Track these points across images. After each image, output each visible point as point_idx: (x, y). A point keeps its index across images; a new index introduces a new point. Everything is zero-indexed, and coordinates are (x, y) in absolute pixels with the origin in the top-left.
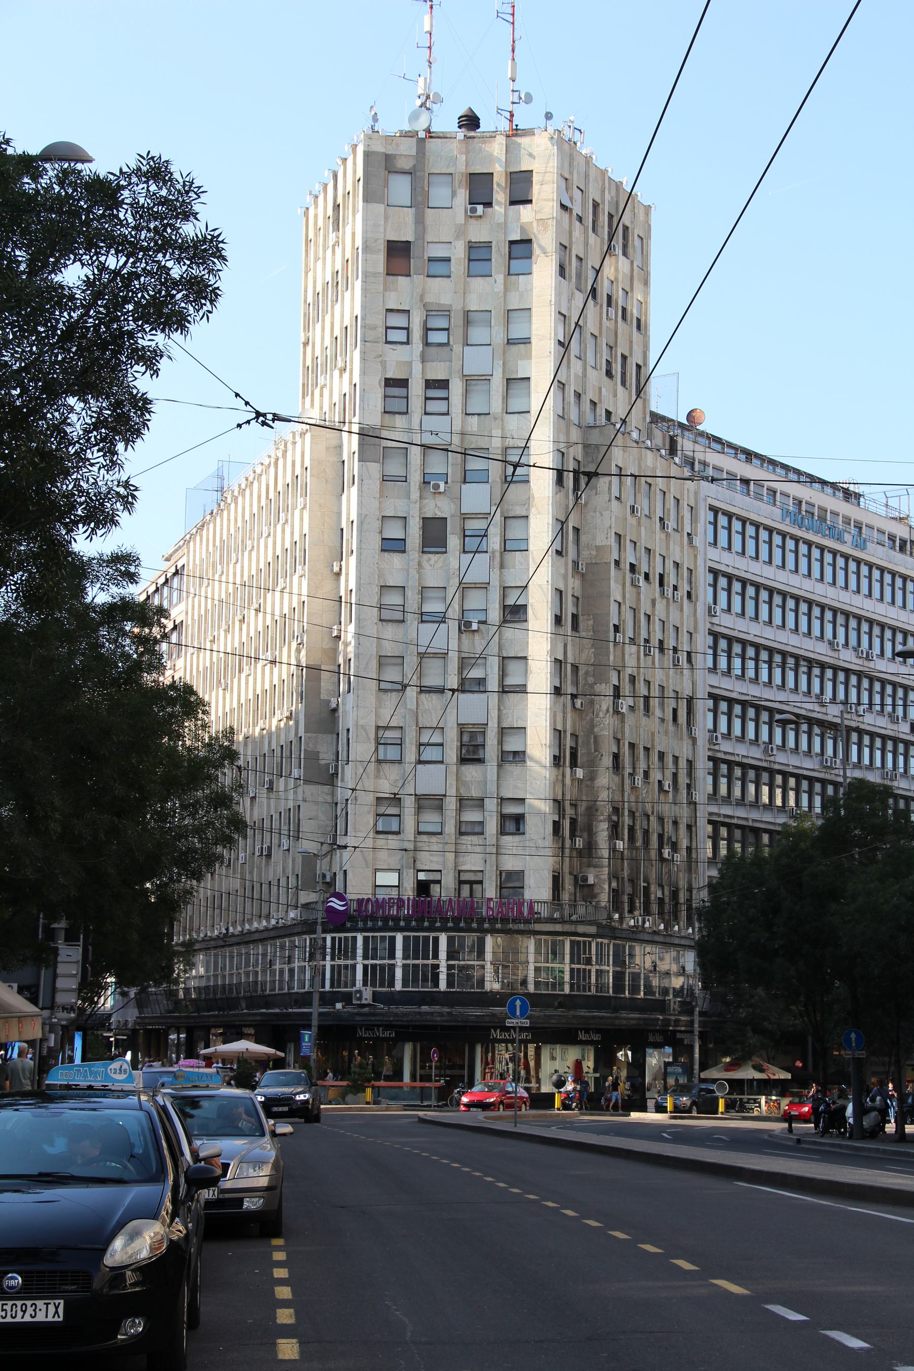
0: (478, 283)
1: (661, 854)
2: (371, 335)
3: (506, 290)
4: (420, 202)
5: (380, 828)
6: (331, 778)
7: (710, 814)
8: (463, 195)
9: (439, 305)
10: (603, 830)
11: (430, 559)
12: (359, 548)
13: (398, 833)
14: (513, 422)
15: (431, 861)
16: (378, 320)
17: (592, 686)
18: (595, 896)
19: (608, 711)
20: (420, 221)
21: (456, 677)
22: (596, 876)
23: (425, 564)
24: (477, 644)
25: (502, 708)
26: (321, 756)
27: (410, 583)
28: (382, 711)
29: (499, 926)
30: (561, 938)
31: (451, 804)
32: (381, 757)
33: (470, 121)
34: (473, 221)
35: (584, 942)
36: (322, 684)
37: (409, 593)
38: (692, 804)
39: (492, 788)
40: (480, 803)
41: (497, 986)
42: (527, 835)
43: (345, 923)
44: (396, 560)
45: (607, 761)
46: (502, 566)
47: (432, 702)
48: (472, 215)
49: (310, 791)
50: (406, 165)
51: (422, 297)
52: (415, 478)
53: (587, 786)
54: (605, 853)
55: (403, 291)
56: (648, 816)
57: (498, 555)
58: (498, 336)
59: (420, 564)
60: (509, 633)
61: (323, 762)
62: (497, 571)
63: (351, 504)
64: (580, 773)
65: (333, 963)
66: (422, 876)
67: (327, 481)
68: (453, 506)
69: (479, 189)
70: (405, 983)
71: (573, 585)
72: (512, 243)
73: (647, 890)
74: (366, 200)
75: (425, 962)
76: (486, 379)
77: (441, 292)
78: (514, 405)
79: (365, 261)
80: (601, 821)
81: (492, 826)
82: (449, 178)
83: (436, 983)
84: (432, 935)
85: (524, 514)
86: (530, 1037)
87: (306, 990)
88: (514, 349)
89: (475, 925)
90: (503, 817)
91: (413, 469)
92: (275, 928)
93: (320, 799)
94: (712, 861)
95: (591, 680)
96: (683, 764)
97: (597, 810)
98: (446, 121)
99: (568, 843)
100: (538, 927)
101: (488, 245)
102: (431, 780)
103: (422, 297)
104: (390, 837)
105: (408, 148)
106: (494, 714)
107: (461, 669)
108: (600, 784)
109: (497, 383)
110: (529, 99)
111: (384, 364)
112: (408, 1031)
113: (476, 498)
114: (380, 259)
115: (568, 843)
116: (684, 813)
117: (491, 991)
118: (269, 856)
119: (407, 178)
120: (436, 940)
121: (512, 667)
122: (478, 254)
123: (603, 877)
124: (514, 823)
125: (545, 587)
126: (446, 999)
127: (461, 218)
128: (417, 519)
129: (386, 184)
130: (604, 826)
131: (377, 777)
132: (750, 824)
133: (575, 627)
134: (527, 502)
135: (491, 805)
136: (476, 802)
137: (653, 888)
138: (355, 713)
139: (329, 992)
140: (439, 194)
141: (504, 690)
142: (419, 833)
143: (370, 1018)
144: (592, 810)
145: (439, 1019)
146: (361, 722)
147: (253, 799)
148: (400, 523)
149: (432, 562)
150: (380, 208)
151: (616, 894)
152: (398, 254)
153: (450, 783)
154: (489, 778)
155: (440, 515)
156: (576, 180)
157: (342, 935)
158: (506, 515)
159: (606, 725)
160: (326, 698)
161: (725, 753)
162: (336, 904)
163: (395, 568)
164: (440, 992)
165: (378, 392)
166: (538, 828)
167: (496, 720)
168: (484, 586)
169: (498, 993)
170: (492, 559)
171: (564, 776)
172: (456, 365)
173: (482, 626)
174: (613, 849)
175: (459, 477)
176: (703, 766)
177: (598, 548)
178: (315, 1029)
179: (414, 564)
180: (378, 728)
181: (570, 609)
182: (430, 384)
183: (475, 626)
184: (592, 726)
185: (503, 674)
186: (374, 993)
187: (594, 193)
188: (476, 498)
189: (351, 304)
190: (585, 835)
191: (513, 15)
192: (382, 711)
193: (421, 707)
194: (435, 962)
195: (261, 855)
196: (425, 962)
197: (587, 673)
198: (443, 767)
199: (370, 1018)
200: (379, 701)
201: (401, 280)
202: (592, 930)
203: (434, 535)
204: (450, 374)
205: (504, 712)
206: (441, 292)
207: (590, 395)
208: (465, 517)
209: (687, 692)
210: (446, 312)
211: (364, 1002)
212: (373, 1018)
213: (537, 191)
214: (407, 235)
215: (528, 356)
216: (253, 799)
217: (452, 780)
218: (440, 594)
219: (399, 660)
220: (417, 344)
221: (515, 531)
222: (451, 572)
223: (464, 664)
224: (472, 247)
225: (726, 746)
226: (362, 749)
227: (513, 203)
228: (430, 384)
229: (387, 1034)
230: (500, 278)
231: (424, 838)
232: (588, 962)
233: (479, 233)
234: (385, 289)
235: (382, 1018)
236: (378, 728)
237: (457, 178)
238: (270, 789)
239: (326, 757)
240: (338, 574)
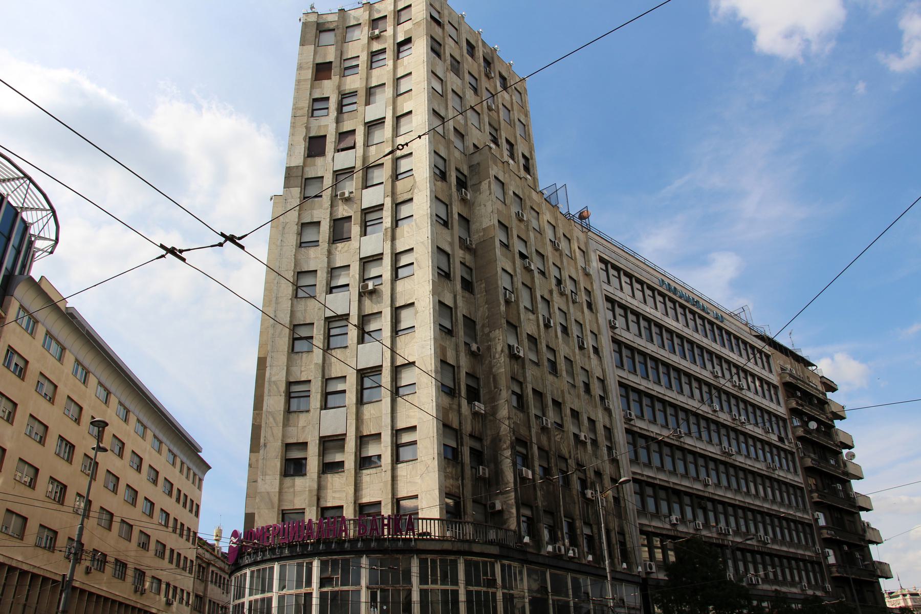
1: (584, 495)
2: (299, 113)
7: (634, 473)
15: (334, 498)
17: (488, 335)
18: (505, 522)
19: (502, 351)
30: (453, 557)
35: (485, 563)
38: (615, 461)
54: (509, 476)
56: (566, 460)
57: (389, 230)
64: (480, 407)
73: (571, 526)
85: (409, 197)
95: (487, 330)
96: (601, 431)
97: (500, 440)
99: (468, 472)
102: (336, 421)
106: (388, 354)
114: (309, 74)
115: (468, 472)
116: (608, 469)
121: (404, 314)
123: (510, 502)
125: (426, 243)
130: (508, 453)
132: (671, 486)
137: (578, 523)
146: (273, 379)
149: (339, 249)
161: (641, 428)
167: (389, 360)
170: (385, 234)
171: (459, 406)
174: (521, 480)
176: (620, 437)
177: (484, 230)
190: (492, 466)
197: (483, 326)
202: (494, 550)
221: (405, 211)
225: (640, 424)
232: (492, 583)
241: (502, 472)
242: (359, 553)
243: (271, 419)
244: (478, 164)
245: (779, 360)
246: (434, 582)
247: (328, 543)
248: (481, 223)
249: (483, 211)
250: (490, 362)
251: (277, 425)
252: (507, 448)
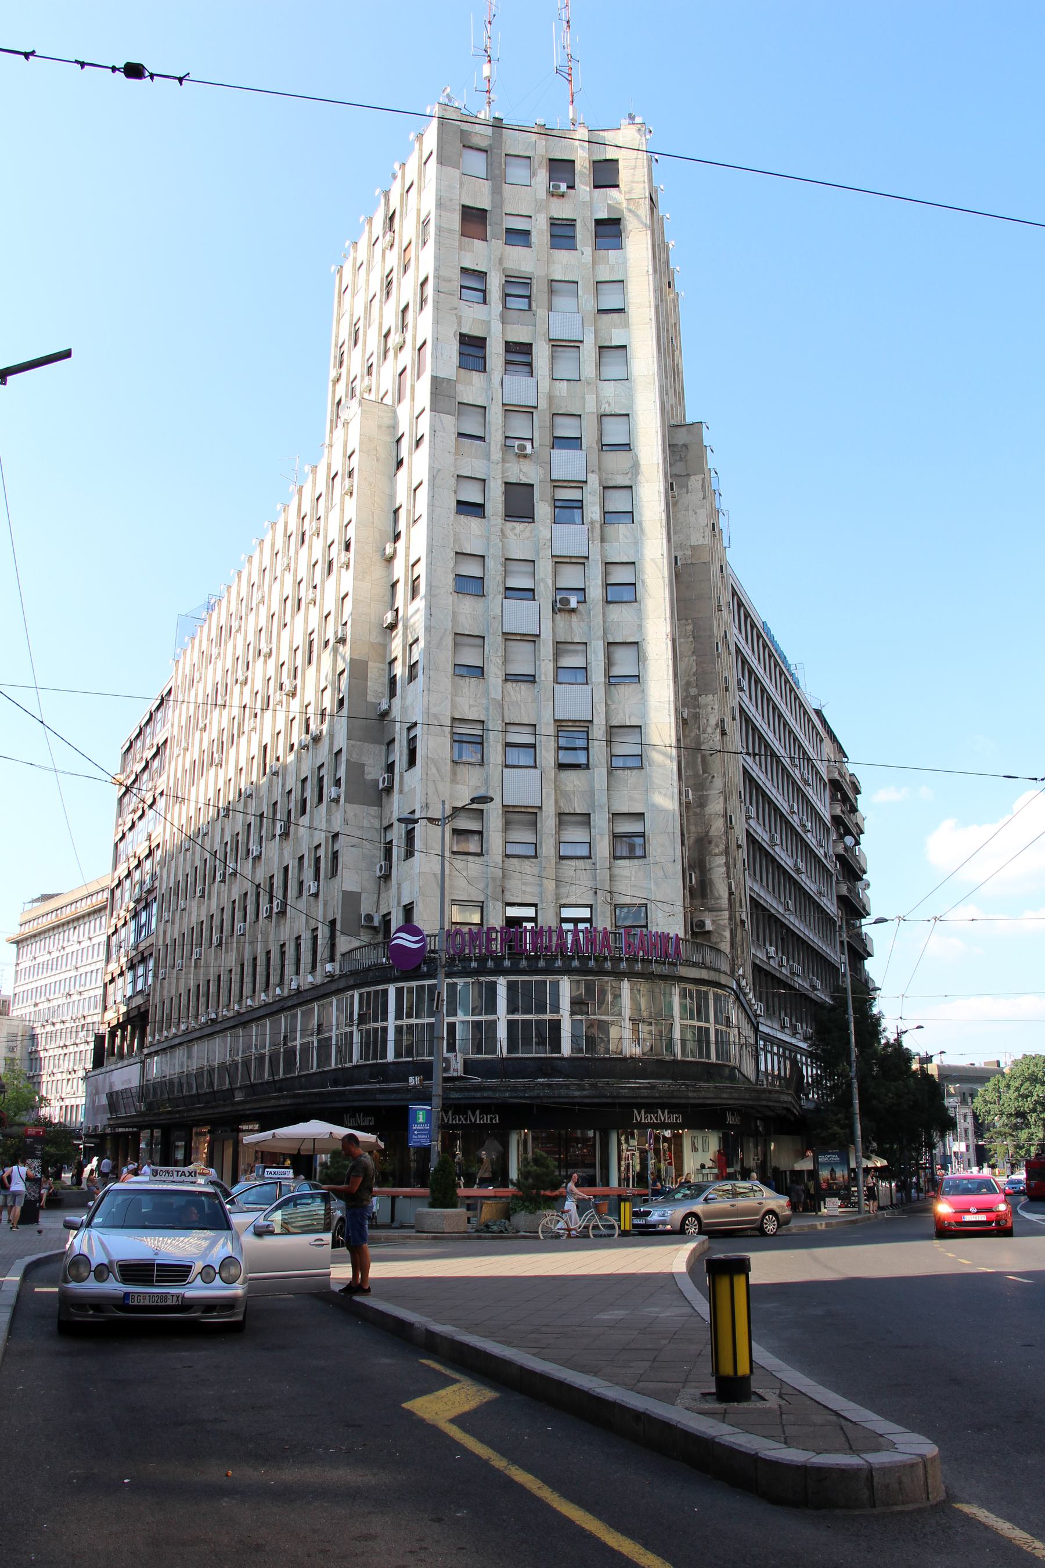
0: (563, 256)
3: (594, 263)
4: (496, 177)
5: (455, 849)
8: (543, 175)
9: (519, 271)
10: (719, 866)
11: (514, 529)
12: (431, 506)
13: (481, 854)
14: (608, 390)
15: (524, 892)
17: (695, 698)
20: (497, 192)
21: (551, 664)
22: (713, 922)
23: (508, 532)
24: (575, 629)
25: (609, 703)
26: (367, 769)
27: (492, 551)
28: (458, 699)
29: (638, 967)
30: (704, 988)
31: (548, 821)
32: (456, 759)
34: (555, 200)
36: (369, 684)
37: (490, 563)
39: (601, 798)
40: (585, 819)
41: (636, 1051)
42: (651, 859)
43: (419, 966)
44: (474, 524)
46: (602, 540)
47: (519, 692)
48: (554, 194)
49: (353, 809)
50: (483, 143)
51: (501, 261)
52: (496, 438)
53: (696, 814)
55: (478, 254)
57: (598, 526)
58: (588, 303)
59: (502, 530)
60: (619, 614)
61: (369, 777)
62: (597, 543)
63: (419, 465)
65: (399, 1023)
66: (513, 912)
67: (378, 460)
68: (541, 471)
69: (561, 169)
70: (512, 1046)
72: (599, 222)
74: (440, 162)
75: (542, 1017)
76: (575, 345)
77: (522, 260)
78: (609, 372)
79: (439, 216)
80: (716, 855)
81: (603, 848)
82: (527, 161)
83: (556, 1046)
84: (549, 979)
85: (627, 483)
86: (680, 1121)
87: (354, 1063)
88: (606, 317)
89: (608, 965)
90: (616, 837)
91: (493, 429)
92: (299, 991)
93: (366, 824)
95: (693, 691)
97: (710, 842)
100: (684, 971)
101: (571, 224)
102: (522, 787)
103: (501, 261)
104: (470, 858)
106: (601, 708)
107: (557, 655)
108: (713, 811)
109: (589, 350)
111: (459, 319)
112: (514, 1115)
113: (567, 464)
114: (455, 220)
117: (631, 1058)
118: (282, 913)
119: (482, 156)
120: (556, 986)
121: (620, 654)
123: (721, 922)
124: (629, 845)
126: (576, 1067)
127: (542, 194)
128: (500, 482)
129: (460, 156)
130: (722, 860)
131: (454, 781)
134: (635, 468)
135: (600, 821)
136: (579, 818)
138: (426, 699)
139: (393, 1063)
140: (516, 173)
141: (611, 680)
142: (507, 856)
143: (473, 1094)
145: (577, 1093)
146: (433, 710)
147: (258, 858)
148: (478, 486)
149: (517, 531)
150: (456, 173)
152: (474, 220)
153: (548, 794)
154: (597, 786)
155: (524, 480)
157: (414, 984)
158: (605, 485)
160: (374, 700)
163: (473, 533)
164: (563, 1059)
165: (453, 347)
166: (666, 849)
167: (603, 716)
168: (581, 562)
169: (640, 1060)
172: (541, 328)
173: (581, 607)
175: (548, 441)
177: (693, 548)
178: (437, 1101)
179: (496, 531)
180: (454, 719)
182: (511, 347)
183: (573, 604)
185: (609, 663)
186: (466, 1062)
188: (567, 464)
191: (570, 75)
192: (458, 699)
193: (507, 699)
194: (555, 1017)
195: (269, 917)
196: (542, 1017)
198: (536, 773)
199: (473, 1094)
200: (453, 683)
201: (478, 243)
203: (519, 503)
204: (534, 338)
205: (613, 707)
206: (522, 260)
208: (557, 484)
210: (526, 282)
211: (452, 1074)
212: (478, 1095)
213: (624, 175)
214: (484, 203)
215: (626, 325)
216: (258, 858)
217: (549, 789)
218: (528, 567)
219: (479, 641)
222: (542, 542)
223: (560, 647)
224: (555, 223)
226: (434, 746)
227: (596, 187)
228: (511, 347)
229: (487, 1119)
230: (588, 250)
231: (515, 861)
233: (562, 210)
234: (461, 248)
235: (491, 1094)
236: (454, 719)
237: (536, 163)
238: (285, 835)
239: (375, 772)
240: (390, 560)
241: (711, 882)
242: (619, 975)
243: (434, 770)
244: (685, 446)
245: (828, 747)
246: (692, 1018)
247: (584, 960)
248: (688, 537)
249: (692, 519)
250: (698, 737)
251: (442, 779)
252: (721, 854)
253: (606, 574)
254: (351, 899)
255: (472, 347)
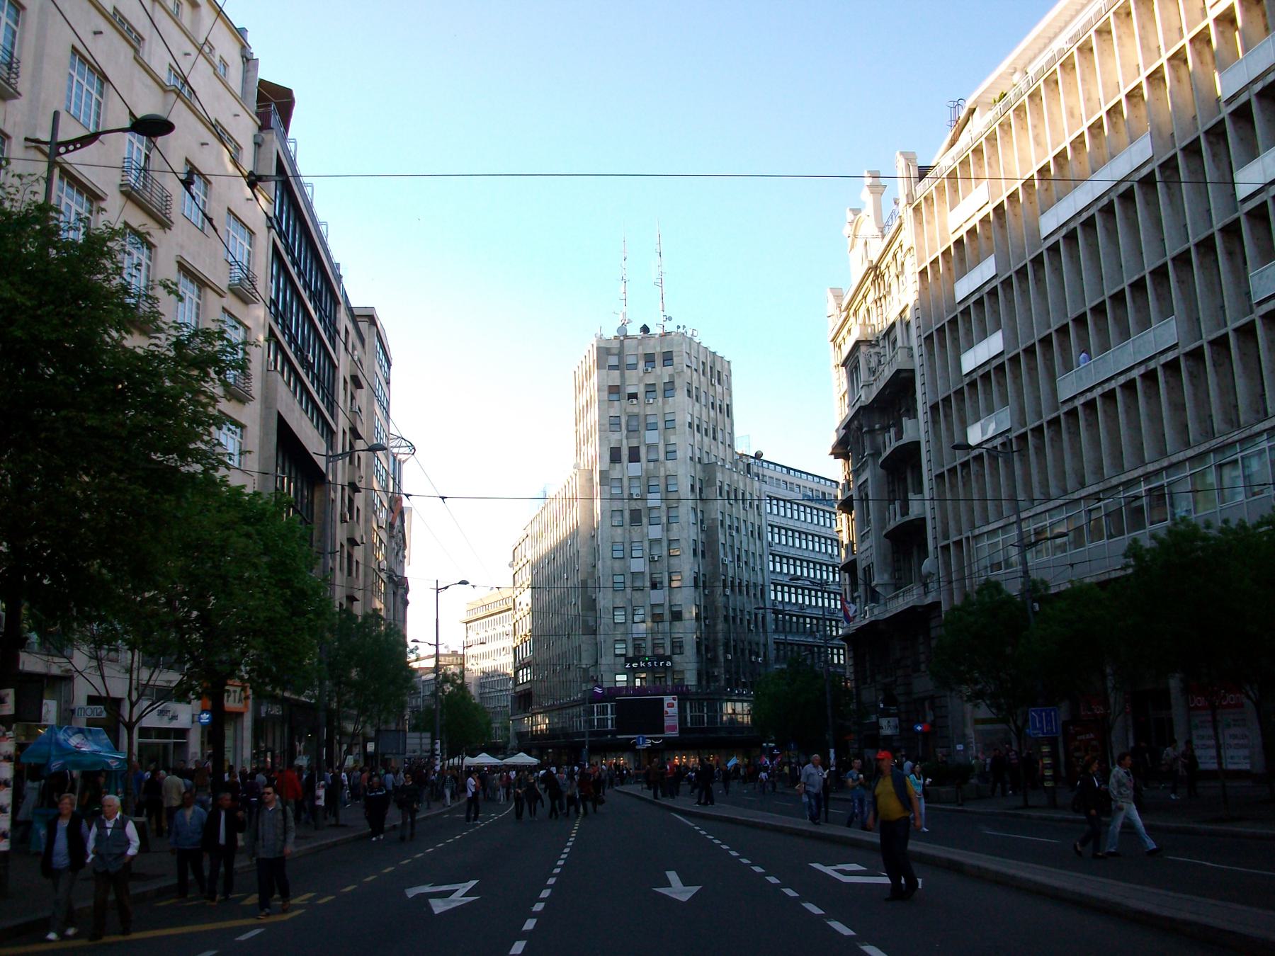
6: (594, 632)
16: (606, 422)
33: (645, 329)
45: (721, 619)
47: (638, 595)
48: (646, 372)
54: (722, 659)
71: (701, 537)
94: (777, 660)
98: (634, 330)
105: (616, 344)
110: (670, 319)
114: (605, 395)
122: (650, 389)
127: (641, 374)
133: (703, 556)
144: (715, 640)
151: (727, 680)
156: (693, 353)
159: (720, 601)
162: (598, 690)
174: (726, 659)
181: (700, 548)
184: (714, 602)
187: (702, 359)
189: (594, 415)
207: (706, 449)
209: (760, 582)
220: (624, 432)
230: (660, 399)
239: (591, 623)
253: (669, 545)
254: (586, 670)
255: (615, 455)
